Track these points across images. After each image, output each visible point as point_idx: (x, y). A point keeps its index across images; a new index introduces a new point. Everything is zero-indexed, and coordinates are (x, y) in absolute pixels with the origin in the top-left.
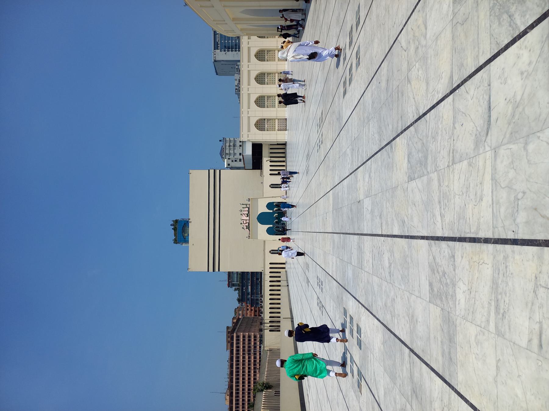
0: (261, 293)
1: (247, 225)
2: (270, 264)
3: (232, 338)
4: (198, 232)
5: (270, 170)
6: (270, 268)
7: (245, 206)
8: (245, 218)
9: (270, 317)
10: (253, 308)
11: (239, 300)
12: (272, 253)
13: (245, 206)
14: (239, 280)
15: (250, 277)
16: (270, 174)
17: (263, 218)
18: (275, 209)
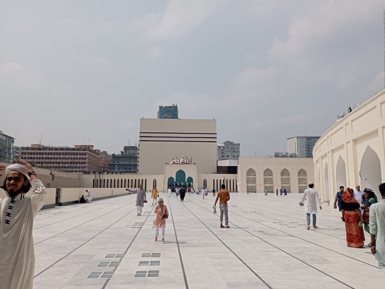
0: (123, 172)
1: (176, 162)
2: (146, 180)
3: (84, 150)
4: (169, 125)
5: (217, 180)
6: (142, 180)
7: (190, 161)
8: (181, 160)
9: (104, 180)
10: (107, 166)
11: (113, 155)
12: (154, 181)
13: (190, 160)
14: (130, 154)
15: (132, 163)
16: (214, 180)
17: (181, 174)
18: (187, 183)
